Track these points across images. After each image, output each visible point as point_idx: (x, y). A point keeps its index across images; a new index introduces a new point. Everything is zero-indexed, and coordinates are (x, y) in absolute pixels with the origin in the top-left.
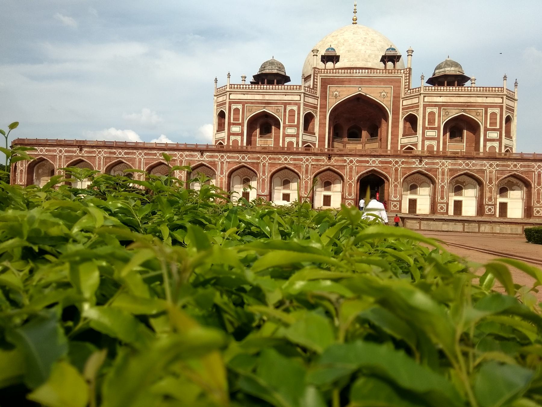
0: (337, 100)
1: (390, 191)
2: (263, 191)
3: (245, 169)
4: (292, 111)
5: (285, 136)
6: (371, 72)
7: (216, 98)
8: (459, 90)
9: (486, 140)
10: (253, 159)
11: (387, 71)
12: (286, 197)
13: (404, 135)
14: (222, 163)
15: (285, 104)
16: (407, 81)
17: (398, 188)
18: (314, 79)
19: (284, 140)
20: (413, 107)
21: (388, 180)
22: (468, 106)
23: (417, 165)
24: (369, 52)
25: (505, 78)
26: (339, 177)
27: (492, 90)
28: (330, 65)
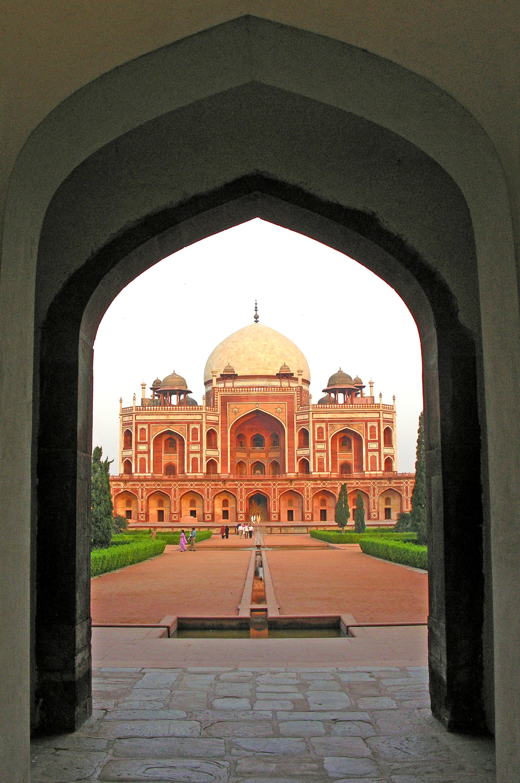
4: (195, 430)
5: (189, 452)
7: (121, 417)
8: (342, 407)
9: (368, 451)
10: (167, 485)
11: (281, 389)
12: (193, 513)
14: (142, 489)
15: (189, 423)
17: (276, 504)
20: (304, 422)
21: (269, 498)
22: (351, 421)
24: (269, 359)
25: (381, 395)
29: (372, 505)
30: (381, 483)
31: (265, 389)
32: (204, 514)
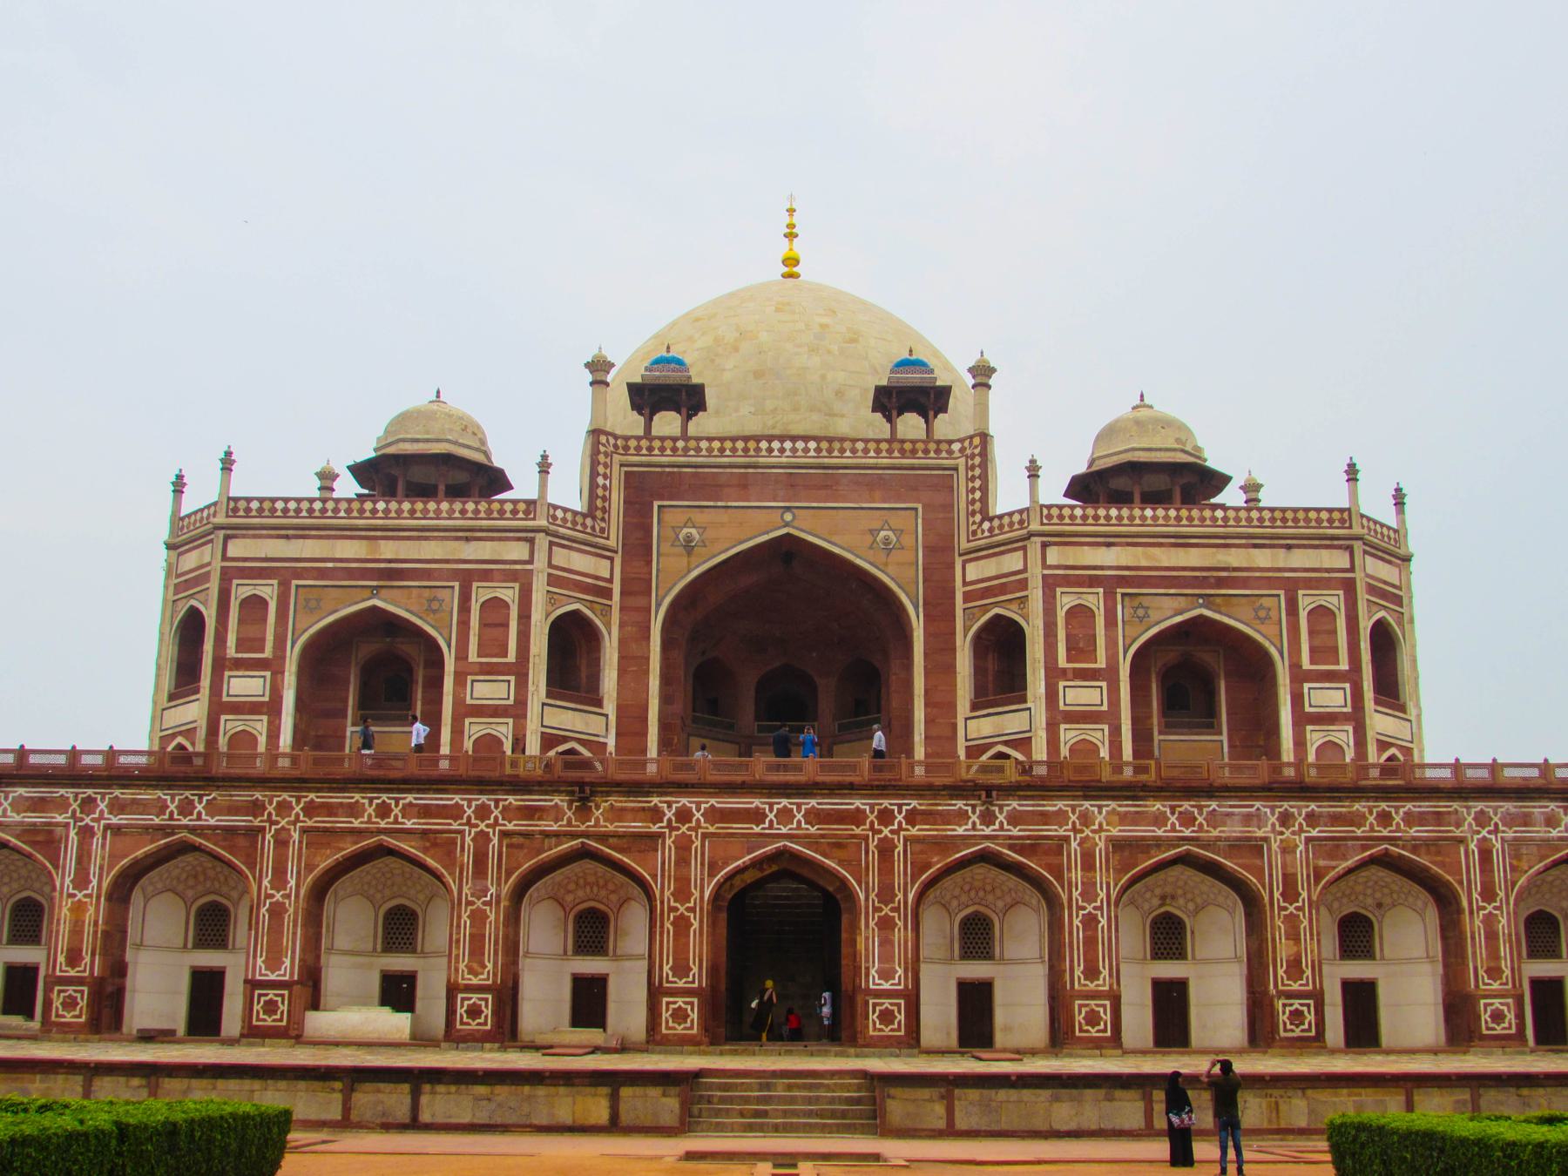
0: (693, 559)
1: (861, 945)
2: (274, 962)
3: (208, 863)
4: (495, 605)
6: (830, 451)
7: (174, 553)
8: (1178, 518)
9: (1302, 719)
10: (233, 810)
11: (896, 446)
12: (398, 992)
13: (974, 707)
14: (86, 833)
15: (467, 579)
16: (978, 483)
17: (898, 936)
18: (594, 474)
19: (458, 732)
20: (1003, 589)
21: (851, 896)
22: (1221, 583)
23: (972, 826)
25: (1352, 473)
26: (636, 891)
27: (1307, 520)
28: (667, 423)
29: (1482, 952)
30: (1526, 820)
31: (824, 445)
32: (452, 990)
